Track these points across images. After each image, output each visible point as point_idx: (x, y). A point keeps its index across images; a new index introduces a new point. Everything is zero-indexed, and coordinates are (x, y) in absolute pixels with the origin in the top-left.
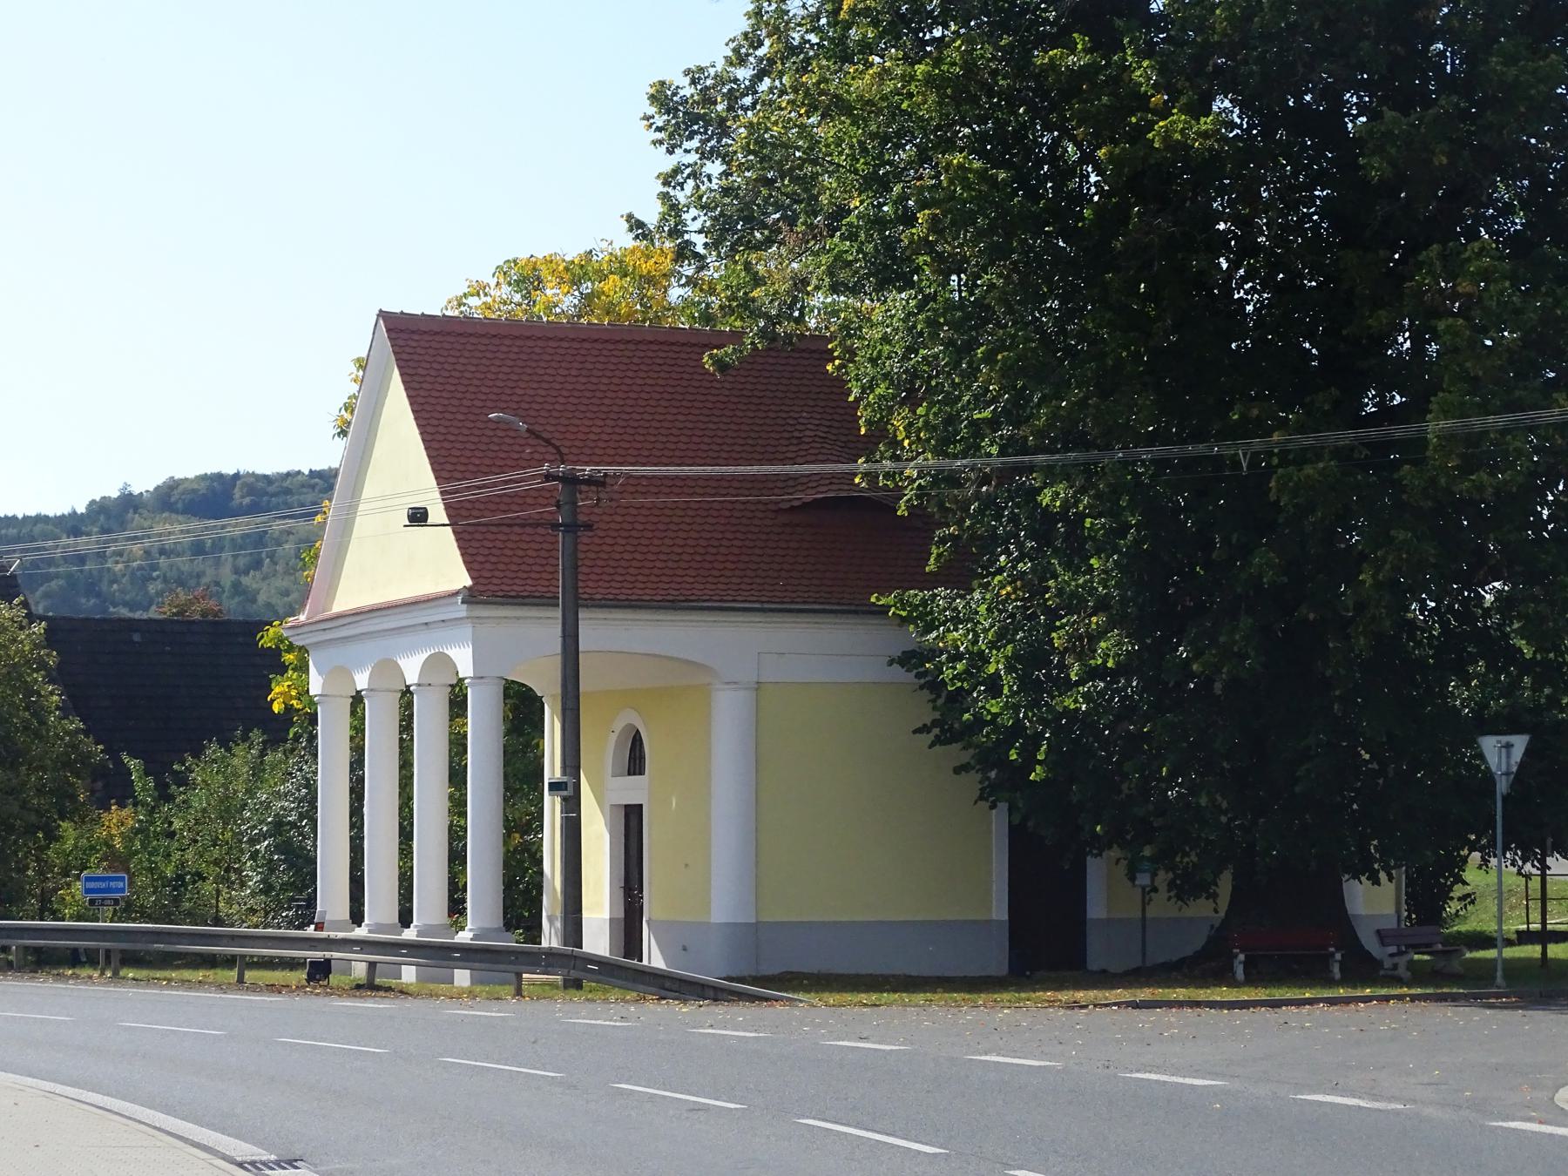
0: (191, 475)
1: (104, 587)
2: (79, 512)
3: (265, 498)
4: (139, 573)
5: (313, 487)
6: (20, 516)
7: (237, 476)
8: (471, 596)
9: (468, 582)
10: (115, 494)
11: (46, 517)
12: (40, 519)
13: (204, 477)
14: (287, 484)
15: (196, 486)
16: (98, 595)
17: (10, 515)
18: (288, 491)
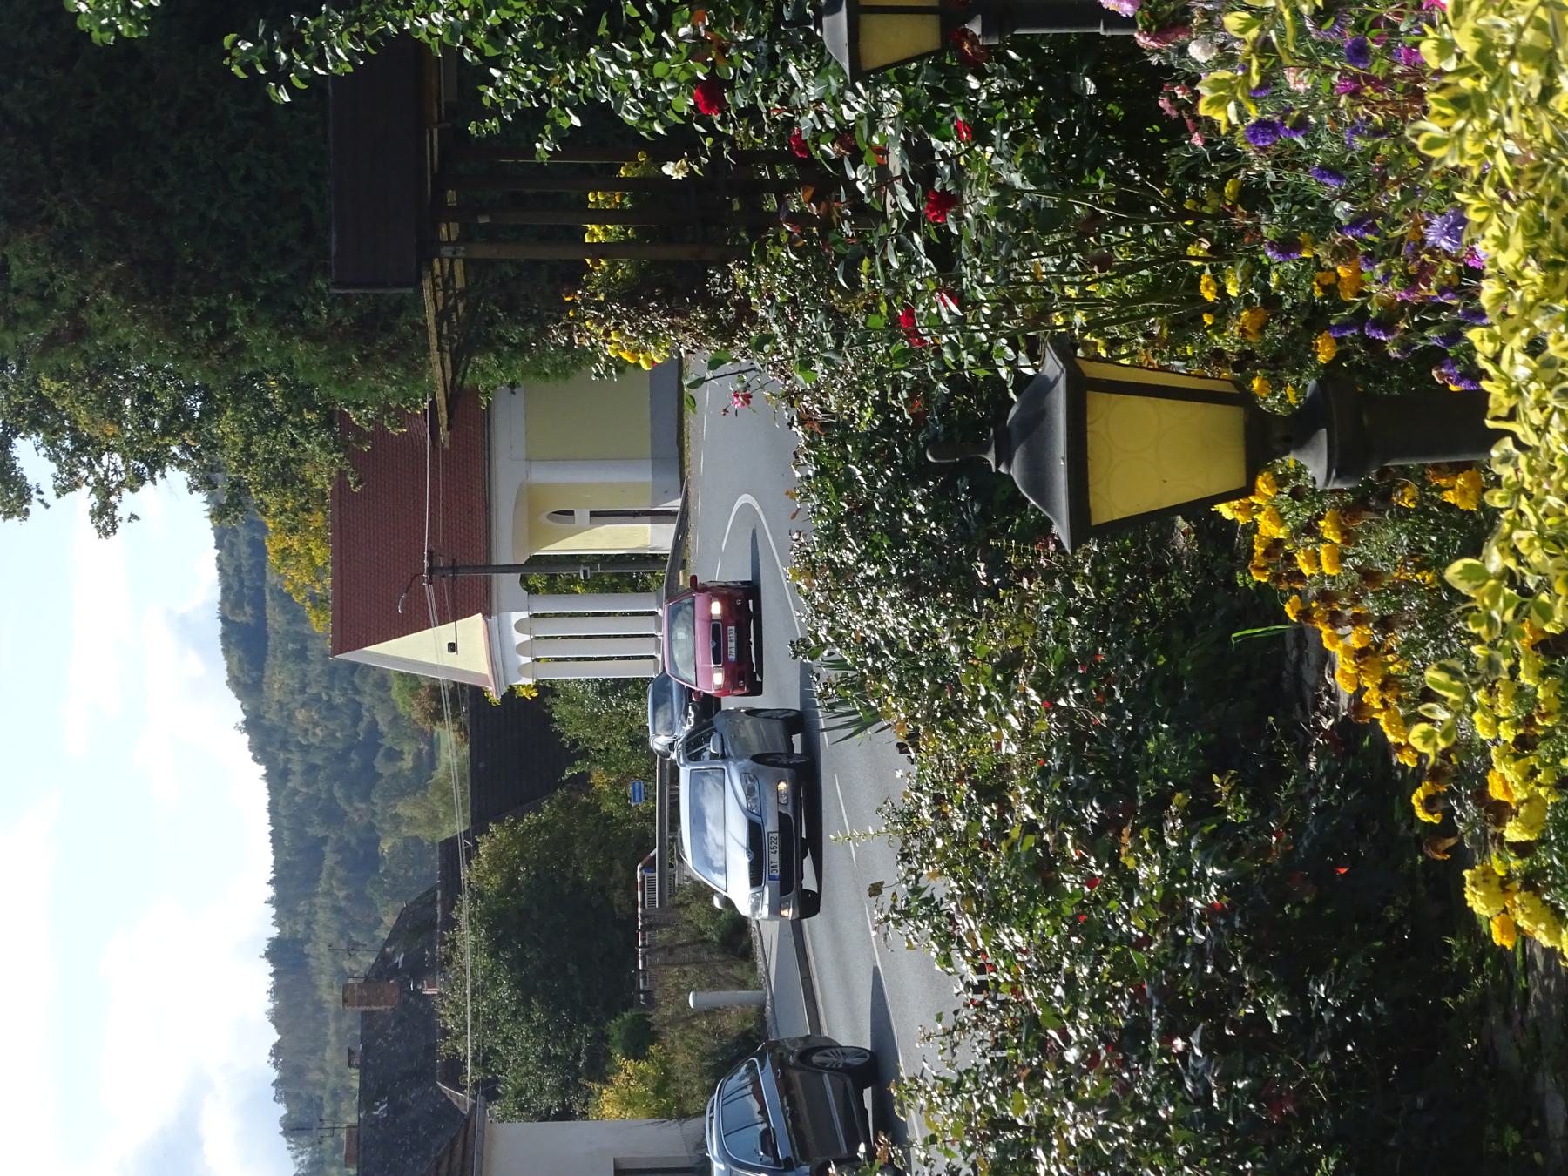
0: (224, 665)
1: (339, 746)
2: (264, 772)
3: (245, 591)
4: (324, 713)
5: (232, 544)
6: (271, 828)
7: (224, 619)
8: (487, 615)
9: (479, 615)
10: (246, 738)
11: (271, 803)
12: (273, 808)
13: (227, 651)
14: (231, 572)
15: (236, 659)
16: (347, 750)
17: (269, 837)
18: (238, 569)
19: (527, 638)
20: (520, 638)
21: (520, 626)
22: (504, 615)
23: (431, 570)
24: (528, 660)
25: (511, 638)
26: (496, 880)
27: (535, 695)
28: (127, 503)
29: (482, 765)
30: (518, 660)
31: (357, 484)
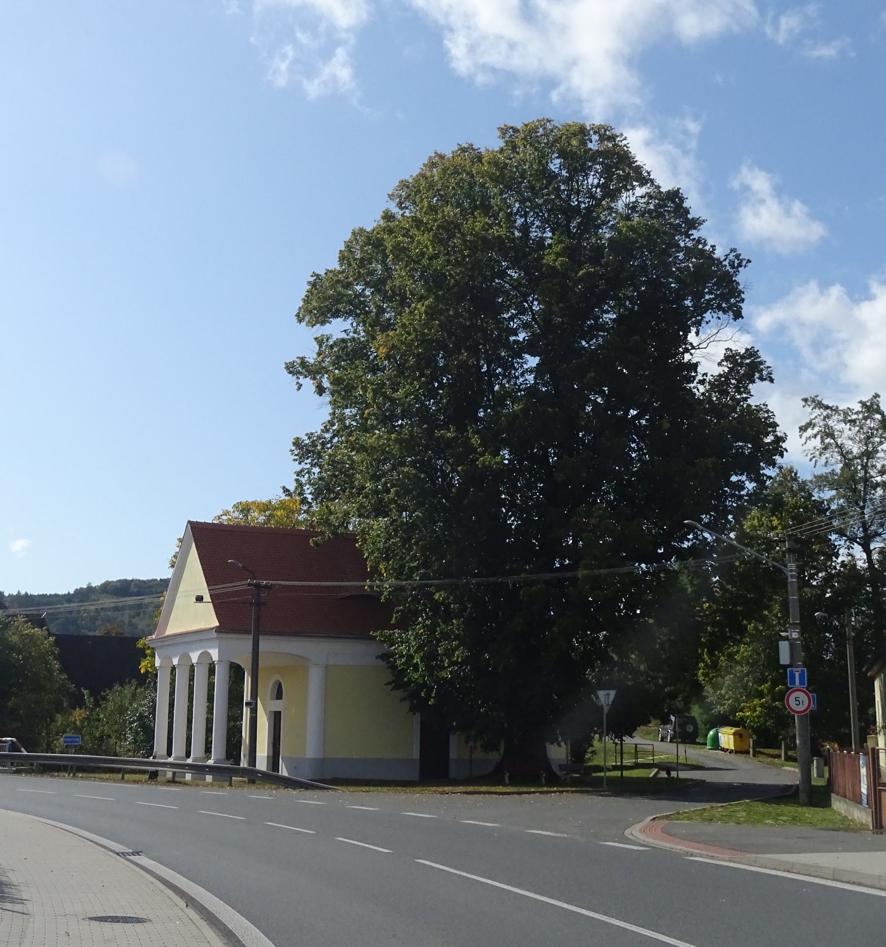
7: (132, 580)
8: (218, 630)
10: (85, 587)
13: (120, 581)
19: (194, 660)
20: (195, 657)
21: (205, 655)
22: (216, 643)
23: (258, 586)
24: (175, 661)
25: (196, 649)
26: (15, 639)
27: (142, 671)
28: (309, 384)
29: (90, 642)
30: (176, 656)
31: (315, 543)
